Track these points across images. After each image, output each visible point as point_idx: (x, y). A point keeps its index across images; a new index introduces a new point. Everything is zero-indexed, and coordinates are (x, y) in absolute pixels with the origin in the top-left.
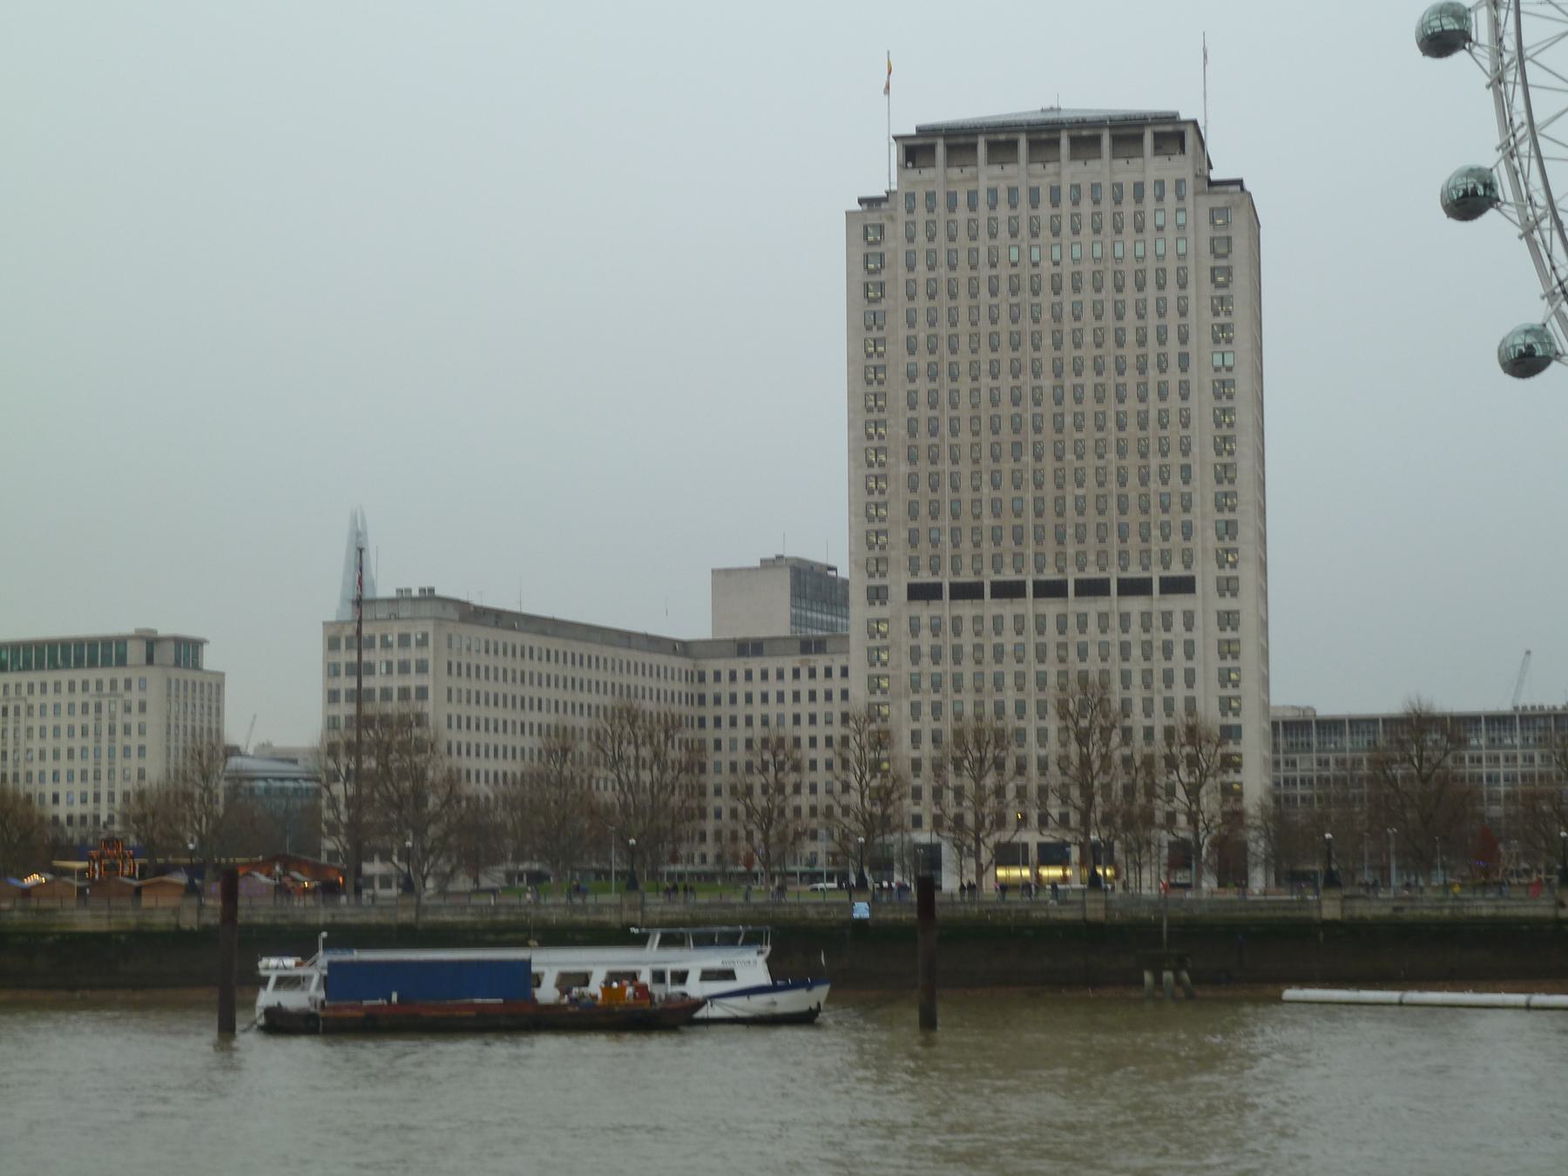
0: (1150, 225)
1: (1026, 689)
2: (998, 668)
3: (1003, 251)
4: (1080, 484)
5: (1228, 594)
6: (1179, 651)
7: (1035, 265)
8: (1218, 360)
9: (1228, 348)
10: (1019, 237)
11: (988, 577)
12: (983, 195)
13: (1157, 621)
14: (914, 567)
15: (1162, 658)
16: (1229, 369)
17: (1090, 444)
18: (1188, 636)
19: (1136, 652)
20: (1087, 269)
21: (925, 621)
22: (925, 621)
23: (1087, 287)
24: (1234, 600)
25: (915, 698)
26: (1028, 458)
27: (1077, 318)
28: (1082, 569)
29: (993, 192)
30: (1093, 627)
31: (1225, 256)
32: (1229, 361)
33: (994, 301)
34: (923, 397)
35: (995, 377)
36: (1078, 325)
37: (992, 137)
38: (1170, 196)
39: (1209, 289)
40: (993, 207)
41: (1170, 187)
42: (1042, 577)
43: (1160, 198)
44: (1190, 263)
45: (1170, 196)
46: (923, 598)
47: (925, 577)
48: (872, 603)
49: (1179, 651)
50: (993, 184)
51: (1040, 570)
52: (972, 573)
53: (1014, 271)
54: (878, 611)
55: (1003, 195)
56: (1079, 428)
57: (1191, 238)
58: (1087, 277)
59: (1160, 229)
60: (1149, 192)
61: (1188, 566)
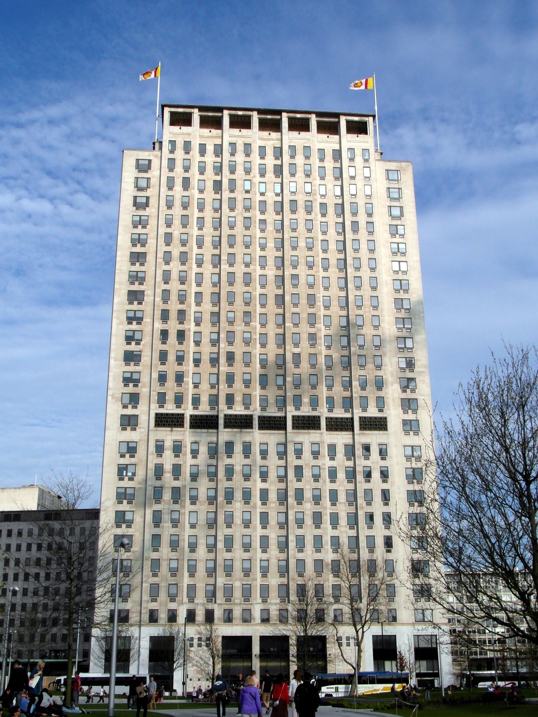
0: (345, 176)
1: (252, 504)
2: (228, 484)
3: (239, 183)
4: (296, 345)
5: (411, 433)
6: (376, 475)
7: (262, 194)
8: (396, 266)
9: (403, 259)
10: (252, 175)
11: (224, 410)
12: (226, 148)
13: (359, 451)
14: (162, 399)
15: (363, 480)
16: (405, 273)
17: (304, 316)
18: (383, 463)
19: (341, 475)
20: (301, 199)
21: (168, 444)
22: (168, 444)
23: (301, 210)
24: (416, 437)
25: (157, 507)
26: (256, 324)
27: (294, 230)
28: (298, 408)
29: (233, 145)
30: (307, 454)
31: (398, 199)
32: (404, 267)
33: (232, 214)
34: (175, 275)
35: (231, 265)
36: (294, 234)
37: (233, 112)
38: (359, 160)
39: (388, 220)
40: (233, 154)
41: (358, 152)
42: (265, 414)
43: (352, 159)
44: (374, 201)
45: (359, 160)
46: (169, 426)
47: (170, 408)
48: (124, 429)
49: (376, 475)
50: (233, 140)
51: (263, 409)
52: (208, 408)
53: (247, 196)
54: (129, 435)
55: (240, 148)
56: (296, 305)
57: (374, 186)
58: (301, 205)
59: (353, 178)
60: (345, 155)
61: (381, 411)
